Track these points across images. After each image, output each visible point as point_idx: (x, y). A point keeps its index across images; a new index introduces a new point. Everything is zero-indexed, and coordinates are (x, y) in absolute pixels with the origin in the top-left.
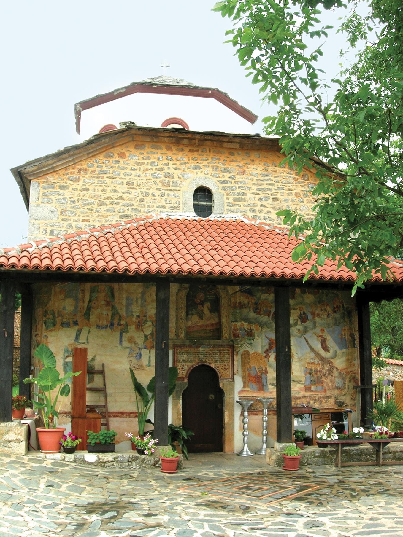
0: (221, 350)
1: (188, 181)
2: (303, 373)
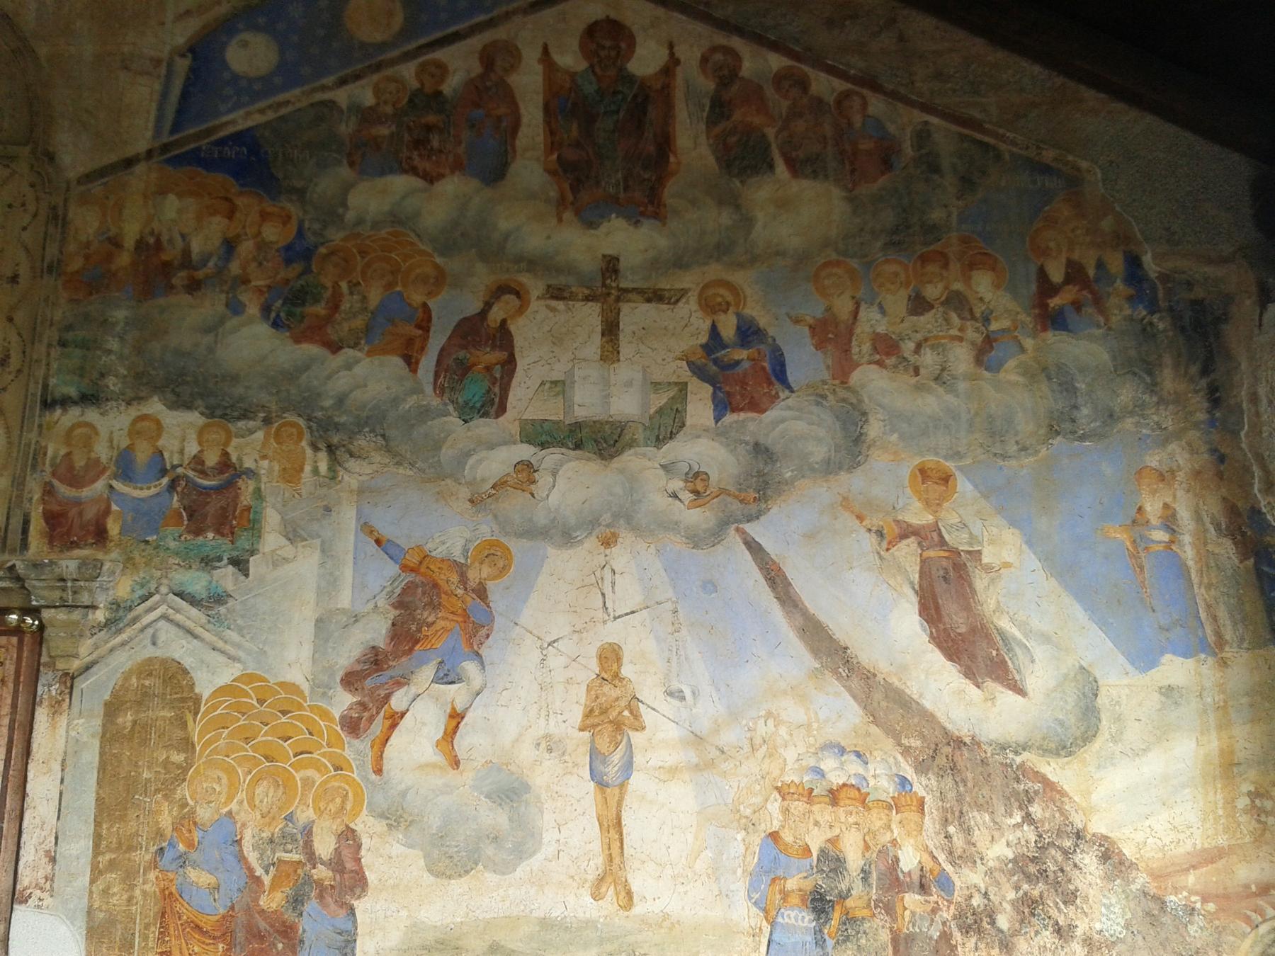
2: (740, 887)
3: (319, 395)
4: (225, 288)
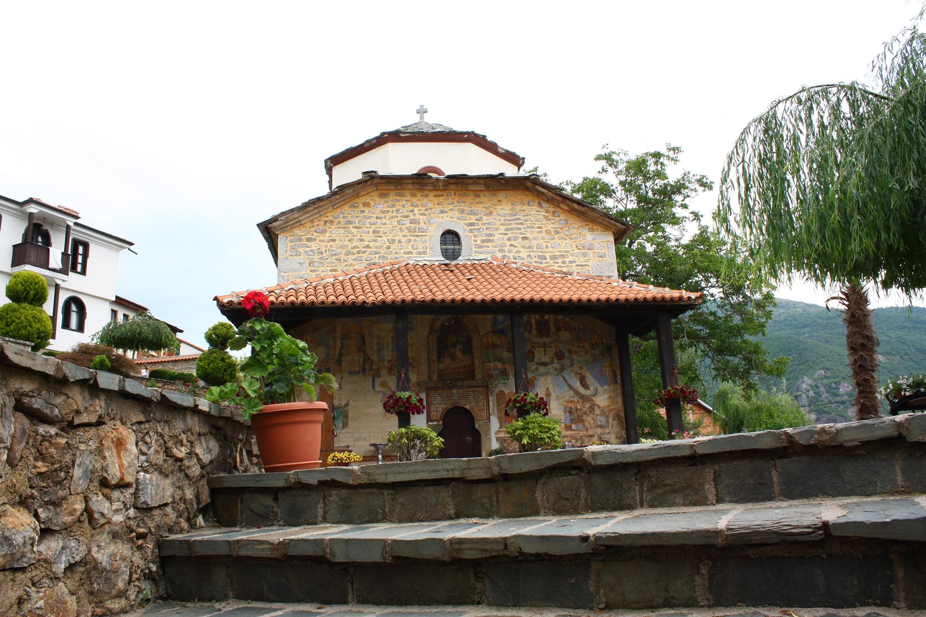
1: (434, 226)
2: (562, 411)
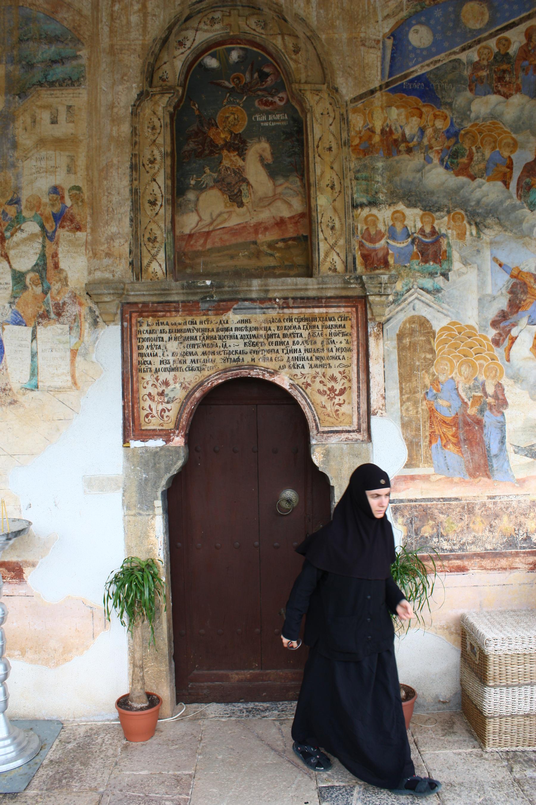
0: (314, 319)
3: (469, 200)
4: (423, 151)
